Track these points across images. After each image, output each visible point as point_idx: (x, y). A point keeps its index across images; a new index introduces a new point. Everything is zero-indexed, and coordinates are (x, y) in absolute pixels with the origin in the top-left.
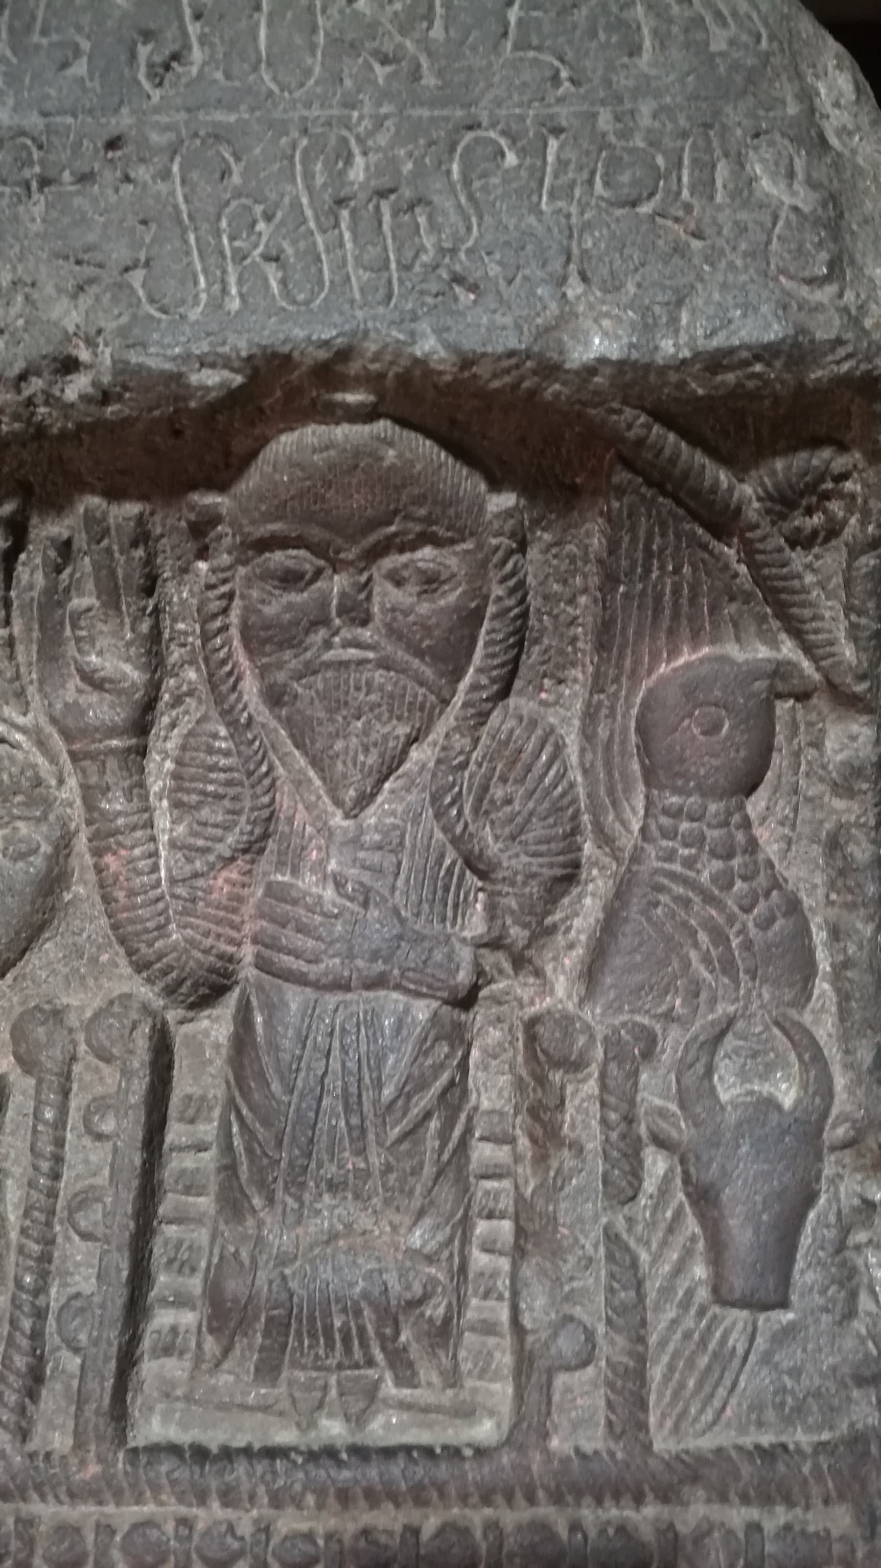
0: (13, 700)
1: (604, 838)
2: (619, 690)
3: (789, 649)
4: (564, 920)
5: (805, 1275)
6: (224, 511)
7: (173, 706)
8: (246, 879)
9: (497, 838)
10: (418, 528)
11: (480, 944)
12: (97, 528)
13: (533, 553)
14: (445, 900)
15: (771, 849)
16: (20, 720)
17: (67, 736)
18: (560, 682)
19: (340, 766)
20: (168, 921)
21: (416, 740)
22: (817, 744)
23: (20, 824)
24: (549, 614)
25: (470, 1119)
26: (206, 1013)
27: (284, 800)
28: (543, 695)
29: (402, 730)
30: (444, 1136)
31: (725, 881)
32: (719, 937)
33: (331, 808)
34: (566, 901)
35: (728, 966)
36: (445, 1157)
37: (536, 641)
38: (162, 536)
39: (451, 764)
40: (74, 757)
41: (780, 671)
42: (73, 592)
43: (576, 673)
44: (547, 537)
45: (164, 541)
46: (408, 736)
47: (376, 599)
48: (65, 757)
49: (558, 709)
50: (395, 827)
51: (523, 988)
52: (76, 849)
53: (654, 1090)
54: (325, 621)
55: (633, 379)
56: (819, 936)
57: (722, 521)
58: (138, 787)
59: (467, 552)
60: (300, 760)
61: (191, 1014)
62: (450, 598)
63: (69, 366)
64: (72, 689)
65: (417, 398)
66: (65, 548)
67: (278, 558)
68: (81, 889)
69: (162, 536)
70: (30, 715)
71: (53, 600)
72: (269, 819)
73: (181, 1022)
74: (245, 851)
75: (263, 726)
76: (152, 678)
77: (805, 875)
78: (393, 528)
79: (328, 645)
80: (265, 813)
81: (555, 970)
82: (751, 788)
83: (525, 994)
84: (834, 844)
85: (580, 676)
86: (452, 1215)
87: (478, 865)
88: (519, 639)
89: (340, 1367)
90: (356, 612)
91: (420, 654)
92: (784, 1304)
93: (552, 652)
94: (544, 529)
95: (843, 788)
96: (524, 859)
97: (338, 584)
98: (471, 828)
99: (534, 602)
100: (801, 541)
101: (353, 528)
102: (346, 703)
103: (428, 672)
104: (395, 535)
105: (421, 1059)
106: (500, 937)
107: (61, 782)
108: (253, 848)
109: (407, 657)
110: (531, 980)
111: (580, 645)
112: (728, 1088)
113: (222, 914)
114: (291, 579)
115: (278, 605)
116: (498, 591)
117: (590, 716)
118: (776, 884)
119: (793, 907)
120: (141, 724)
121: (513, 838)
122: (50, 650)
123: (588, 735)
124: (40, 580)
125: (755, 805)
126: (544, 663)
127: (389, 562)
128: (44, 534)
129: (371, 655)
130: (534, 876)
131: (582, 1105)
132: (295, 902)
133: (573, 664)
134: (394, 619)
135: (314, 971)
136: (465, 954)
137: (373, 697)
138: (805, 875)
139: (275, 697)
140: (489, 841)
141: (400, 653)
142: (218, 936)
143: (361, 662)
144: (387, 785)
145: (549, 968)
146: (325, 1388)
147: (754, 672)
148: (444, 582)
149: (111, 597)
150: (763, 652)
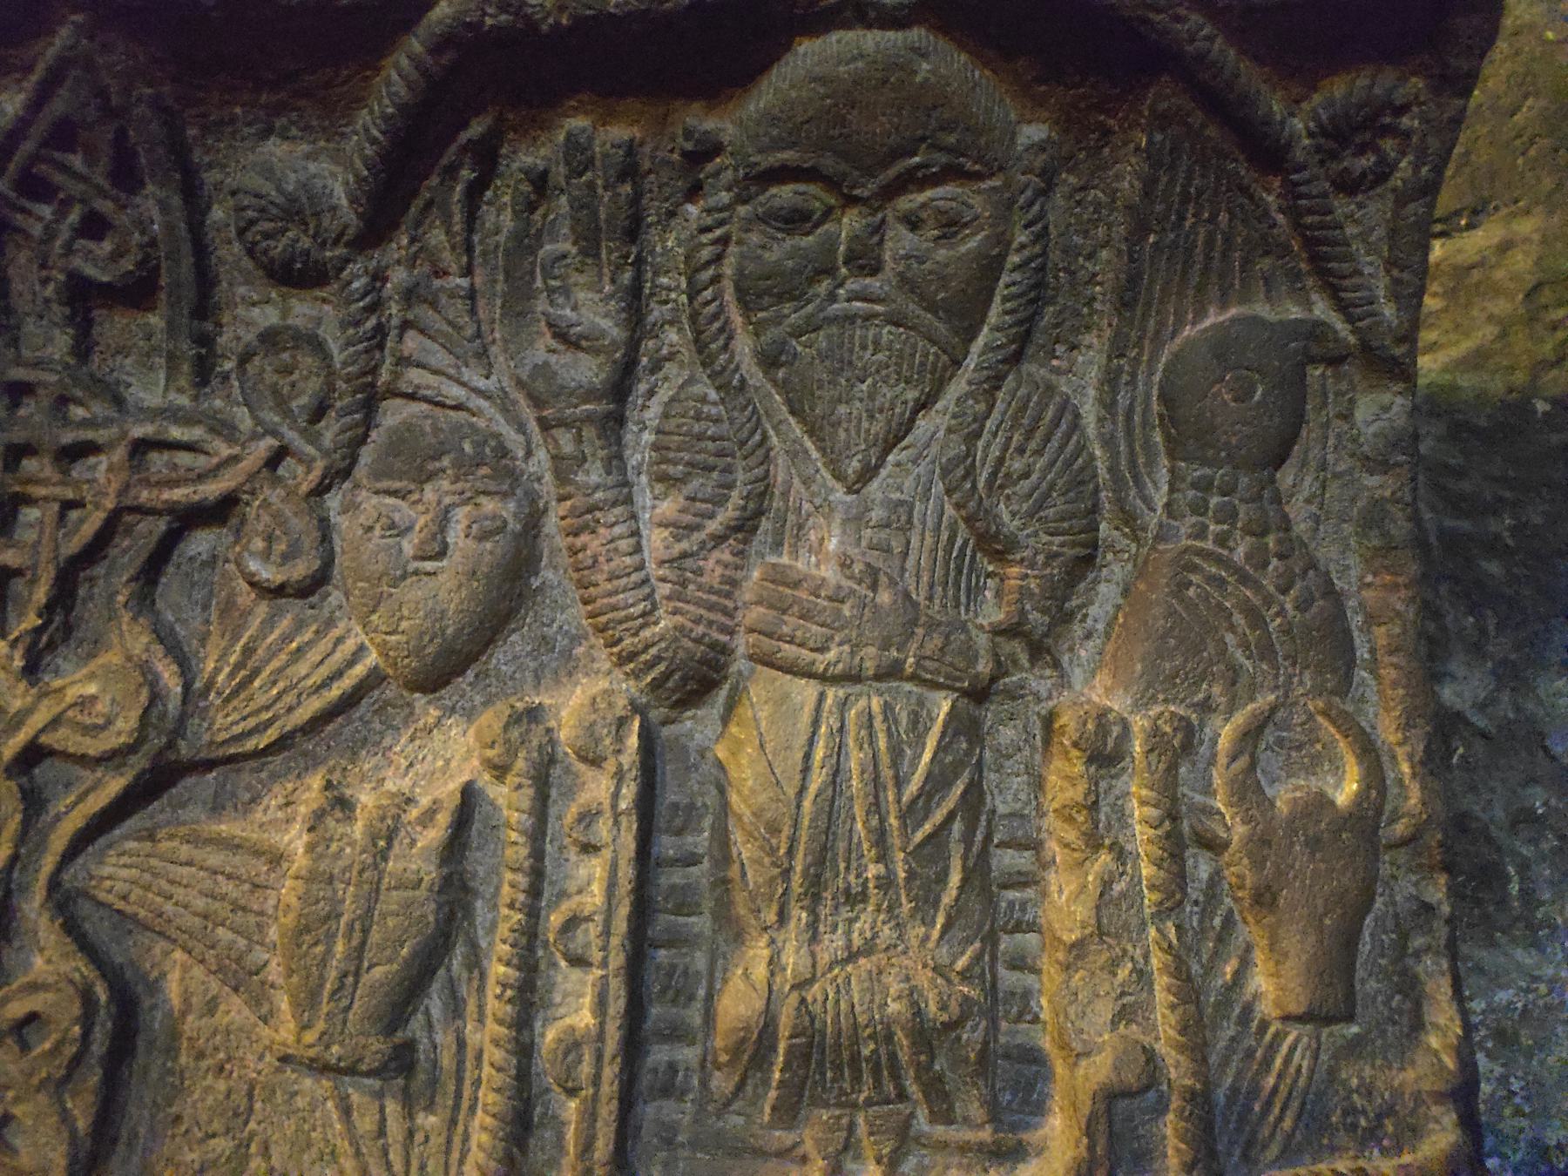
0: (472, 361)
1: (1128, 519)
2: (1140, 354)
3: (1322, 309)
4: (1080, 607)
5: (1368, 985)
6: (726, 139)
7: (652, 372)
8: (738, 560)
9: (1013, 514)
10: (943, 158)
11: (997, 631)
12: (578, 155)
13: (1058, 198)
14: (960, 581)
15: (1301, 528)
16: (481, 383)
17: (537, 402)
18: (1073, 347)
19: (842, 435)
20: (654, 607)
21: (924, 406)
22: (1347, 416)
23: (483, 500)
24: (1065, 270)
25: (989, 822)
26: (689, 714)
27: (780, 471)
28: (1055, 362)
29: (912, 395)
30: (967, 839)
31: (1259, 559)
32: (1255, 618)
33: (831, 482)
34: (1082, 585)
35: (1266, 651)
36: (971, 863)
37: (1052, 301)
38: (650, 171)
40: (545, 426)
41: (1316, 331)
42: (546, 237)
43: (1089, 338)
44: (1072, 180)
45: (652, 177)
46: (917, 400)
47: (889, 244)
48: (533, 426)
49: (1081, 375)
50: (901, 503)
51: (1039, 681)
52: (546, 530)
54: (829, 271)
56: (1356, 620)
57: (1269, 154)
58: (615, 462)
59: (994, 188)
60: (797, 429)
61: (673, 714)
64: (541, 348)
66: (540, 182)
67: (784, 194)
69: (650, 171)
70: (494, 378)
71: (525, 242)
72: (762, 495)
73: (664, 723)
74: (737, 529)
75: (757, 389)
76: (632, 337)
78: (917, 159)
79: (832, 297)
80: (761, 487)
81: (1071, 661)
82: (1279, 461)
83: (1043, 687)
84: (1373, 518)
85: (1095, 341)
86: (980, 928)
87: (996, 546)
88: (1036, 295)
89: (869, 1103)
90: (865, 260)
91: (932, 308)
92: (1350, 1018)
93: (1067, 315)
94: (1069, 171)
95: (1378, 464)
96: (1046, 538)
97: (850, 223)
98: (986, 503)
99: (1055, 256)
100: (1349, 186)
102: (850, 363)
103: (942, 328)
104: (919, 167)
105: (941, 755)
106: (1019, 624)
107: (529, 454)
108: (745, 527)
109: (919, 312)
110: (1048, 672)
111: (1097, 306)
113: (714, 598)
114: (796, 220)
115: (781, 250)
116: (1022, 237)
117: (1111, 380)
118: (1312, 565)
119: (1330, 591)
120: (620, 388)
121: (1031, 515)
123: (1108, 405)
124: (507, 221)
125: (1286, 477)
126: (1057, 325)
127: (910, 201)
128: (515, 166)
129: (879, 308)
130: (1056, 555)
132: (796, 585)
133: (1088, 328)
134: (909, 267)
135: (821, 661)
136: (982, 640)
137: (880, 356)
140: (1007, 517)
141: (911, 306)
142: (710, 623)
143: (869, 317)
144: (890, 458)
145: (1065, 658)
146: (852, 1127)
148: (966, 225)
149: (589, 243)
150: (1295, 312)
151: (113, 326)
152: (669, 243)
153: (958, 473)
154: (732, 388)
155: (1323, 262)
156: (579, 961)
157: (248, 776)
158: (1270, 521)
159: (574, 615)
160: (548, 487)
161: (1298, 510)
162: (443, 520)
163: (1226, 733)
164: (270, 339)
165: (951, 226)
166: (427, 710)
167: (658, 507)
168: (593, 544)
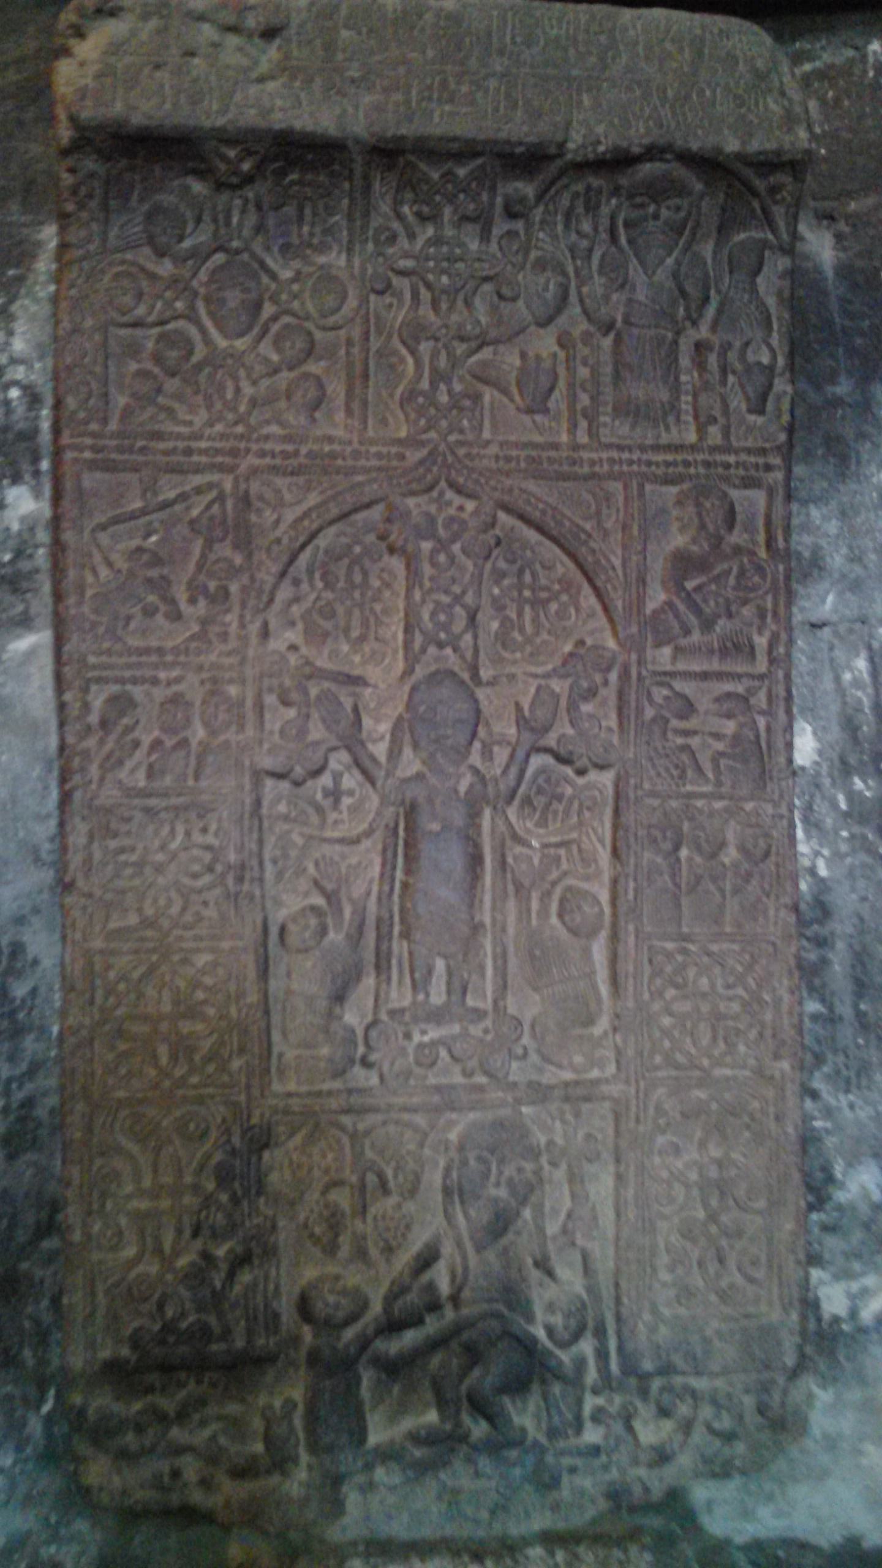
27: (631, 272)
39: (678, 263)
53: (732, 356)
55: (739, 156)
57: (755, 194)
62: (683, 214)
63: (599, 142)
64: (574, 237)
65: (687, 158)
66: (576, 195)
67: (638, 200)
68: (573, 298)
77: (771, 302)
87: (683, 293)
100: (776, 202)
101: (657, 191)
112: (751, 357)
115: (635, 214)
117: (715, 253)
120: (590, 250)
122: (567, 226)
123: (714, 259)
131: (713, 360)
138: (771, 302)
139: (630, 242)
147: (760, 240)
149: (587, 209)
150: (761, 235)
151: (469, 227)
152: (605, 211)
153: (675, 275)
154: (621, 250)
155: (770, 222)
156: (585, 390)
157: (501, 348)
158: (754, 290)
159: (578, 310)
160: (572, 275)
161: (762, 289)
162: (548, 281)
163: (738, 344)
164: (509, 232)
165: (678, 209)
166: (542, 331)
167: (598, 280)
168: (585, 290)
